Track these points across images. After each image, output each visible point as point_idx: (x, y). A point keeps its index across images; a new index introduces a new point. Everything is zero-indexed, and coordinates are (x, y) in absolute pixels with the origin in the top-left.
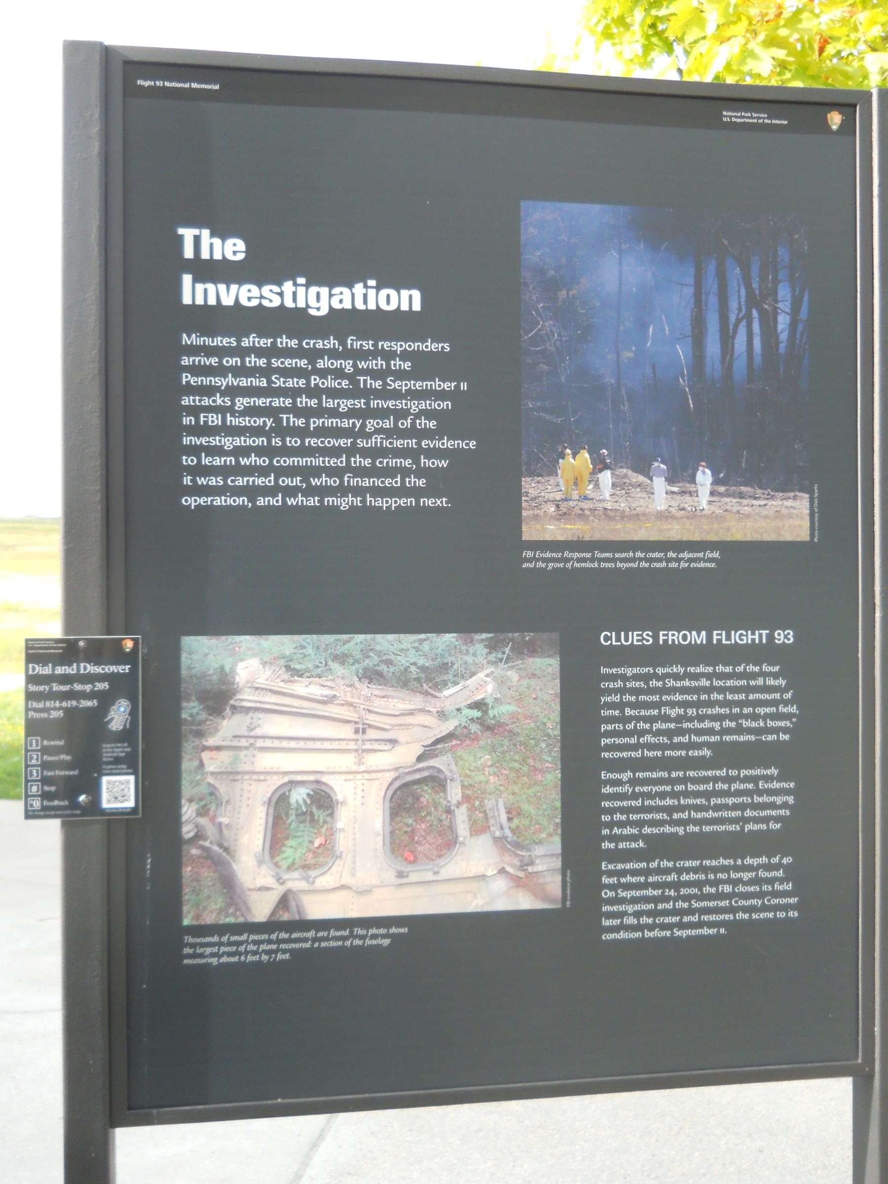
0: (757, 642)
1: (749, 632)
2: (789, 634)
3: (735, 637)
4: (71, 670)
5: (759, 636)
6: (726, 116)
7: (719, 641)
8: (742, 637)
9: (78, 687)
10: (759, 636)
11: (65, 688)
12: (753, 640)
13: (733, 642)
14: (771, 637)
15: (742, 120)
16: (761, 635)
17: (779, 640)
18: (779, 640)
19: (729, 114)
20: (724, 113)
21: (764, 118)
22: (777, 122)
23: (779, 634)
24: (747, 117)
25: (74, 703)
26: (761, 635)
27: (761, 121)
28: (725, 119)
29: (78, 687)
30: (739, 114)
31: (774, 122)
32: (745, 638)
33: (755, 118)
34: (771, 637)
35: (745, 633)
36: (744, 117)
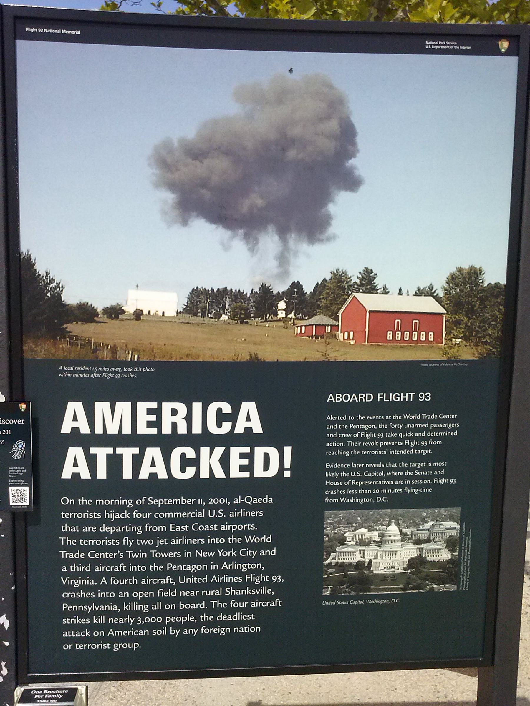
0: (407, 400)
1: (402, 394)
2: (428, 395)
3: (392, 397)
5: (408, 396)
6: (429, 45)
7: (382, 400)
8: (396, 397)
10: (408, 396)
12: (404, 399)
13: (391, 400)
14: (416, 397)
15: (439, 47)
16: (409, 396)
17: (421, 399)
18: (421, 399)
19: (430, 43)
20: (427, 42)
21: (455, 45)
22: (464, 48)
23: (422, 395)
26: (409, 396)
28: (427, 47)
30: (437, 43)
31: (461, 47)
32: (399, 398)
34: (416, 397)
35: (399, 395)
36: (440, 45)
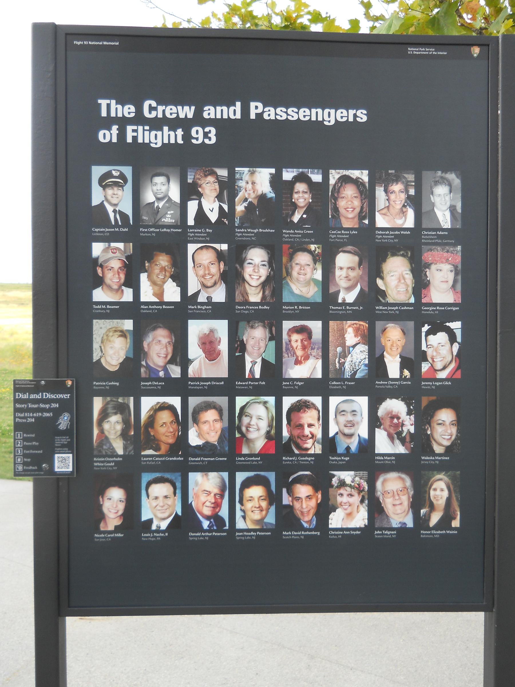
4: (38, 396)
9: (42, 406)
11: (36, 406)
15: (420, 53)
21: (433, 51)
24: (423, 51)
25: (40, 414)
27: (431, 53)
29: (42, 406)
31: (438, 53)
33: (427, 51)
36: (420, 51)
